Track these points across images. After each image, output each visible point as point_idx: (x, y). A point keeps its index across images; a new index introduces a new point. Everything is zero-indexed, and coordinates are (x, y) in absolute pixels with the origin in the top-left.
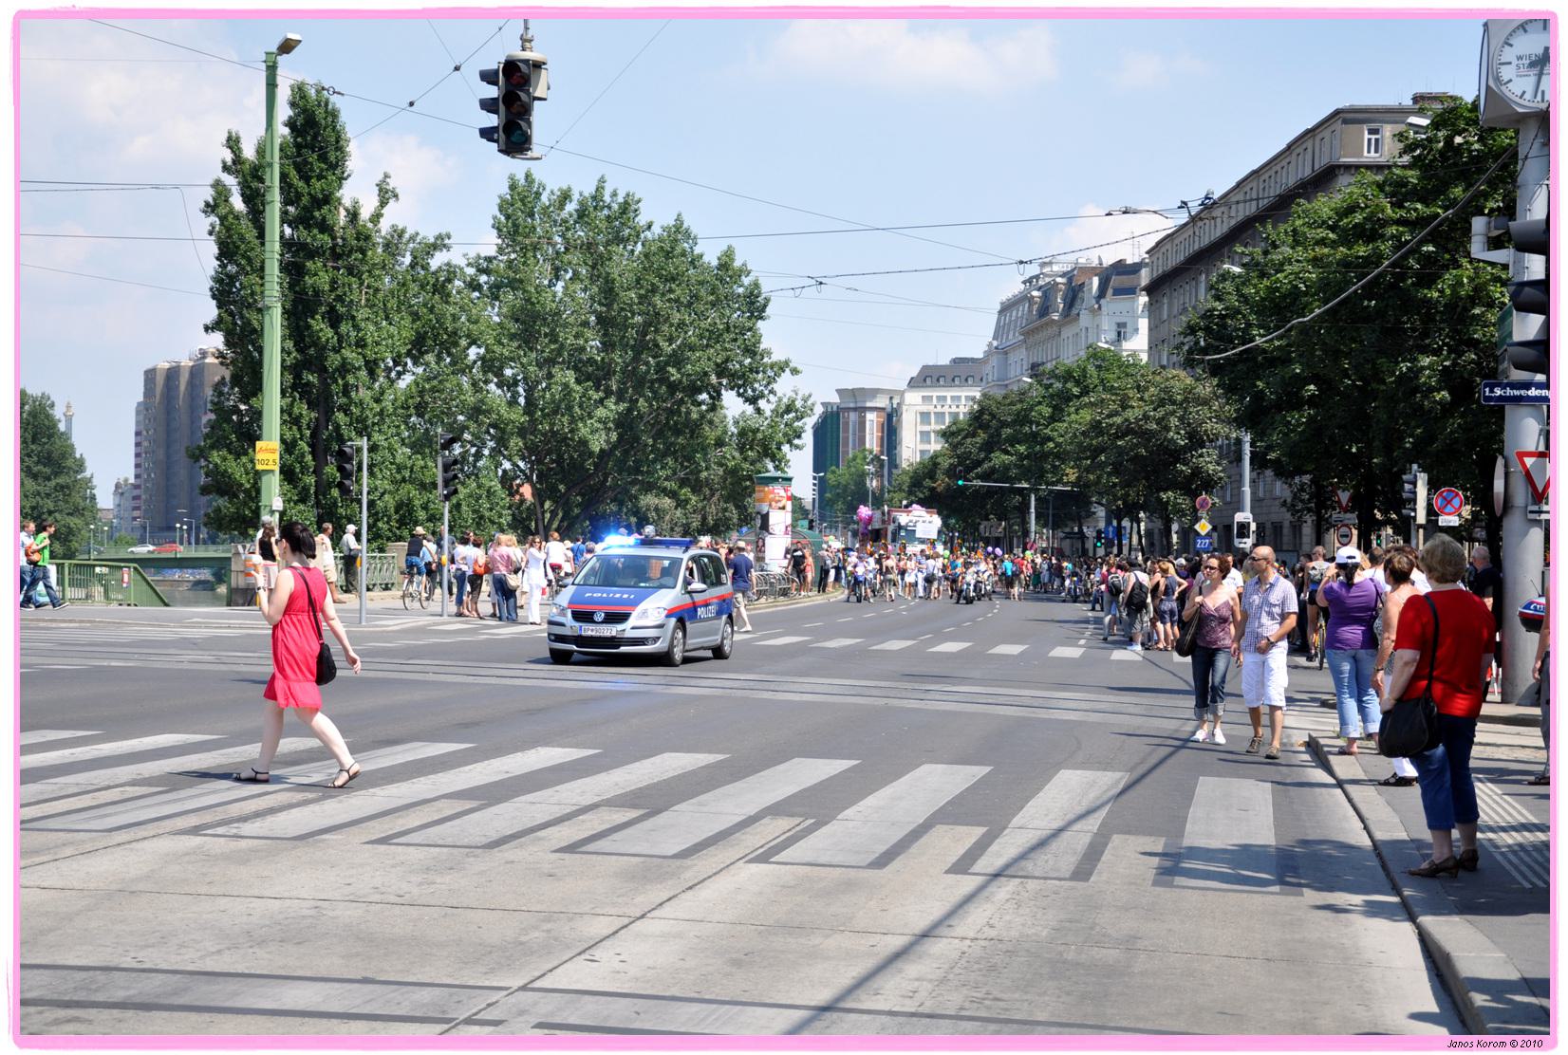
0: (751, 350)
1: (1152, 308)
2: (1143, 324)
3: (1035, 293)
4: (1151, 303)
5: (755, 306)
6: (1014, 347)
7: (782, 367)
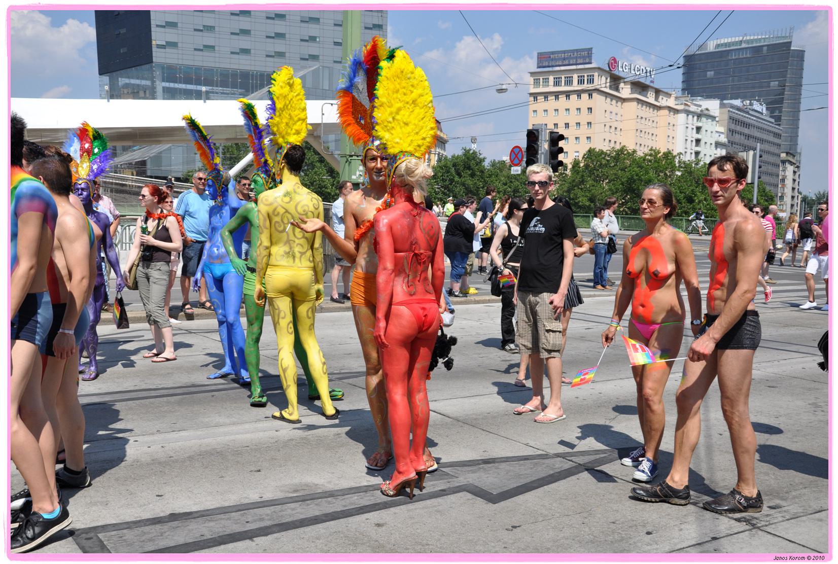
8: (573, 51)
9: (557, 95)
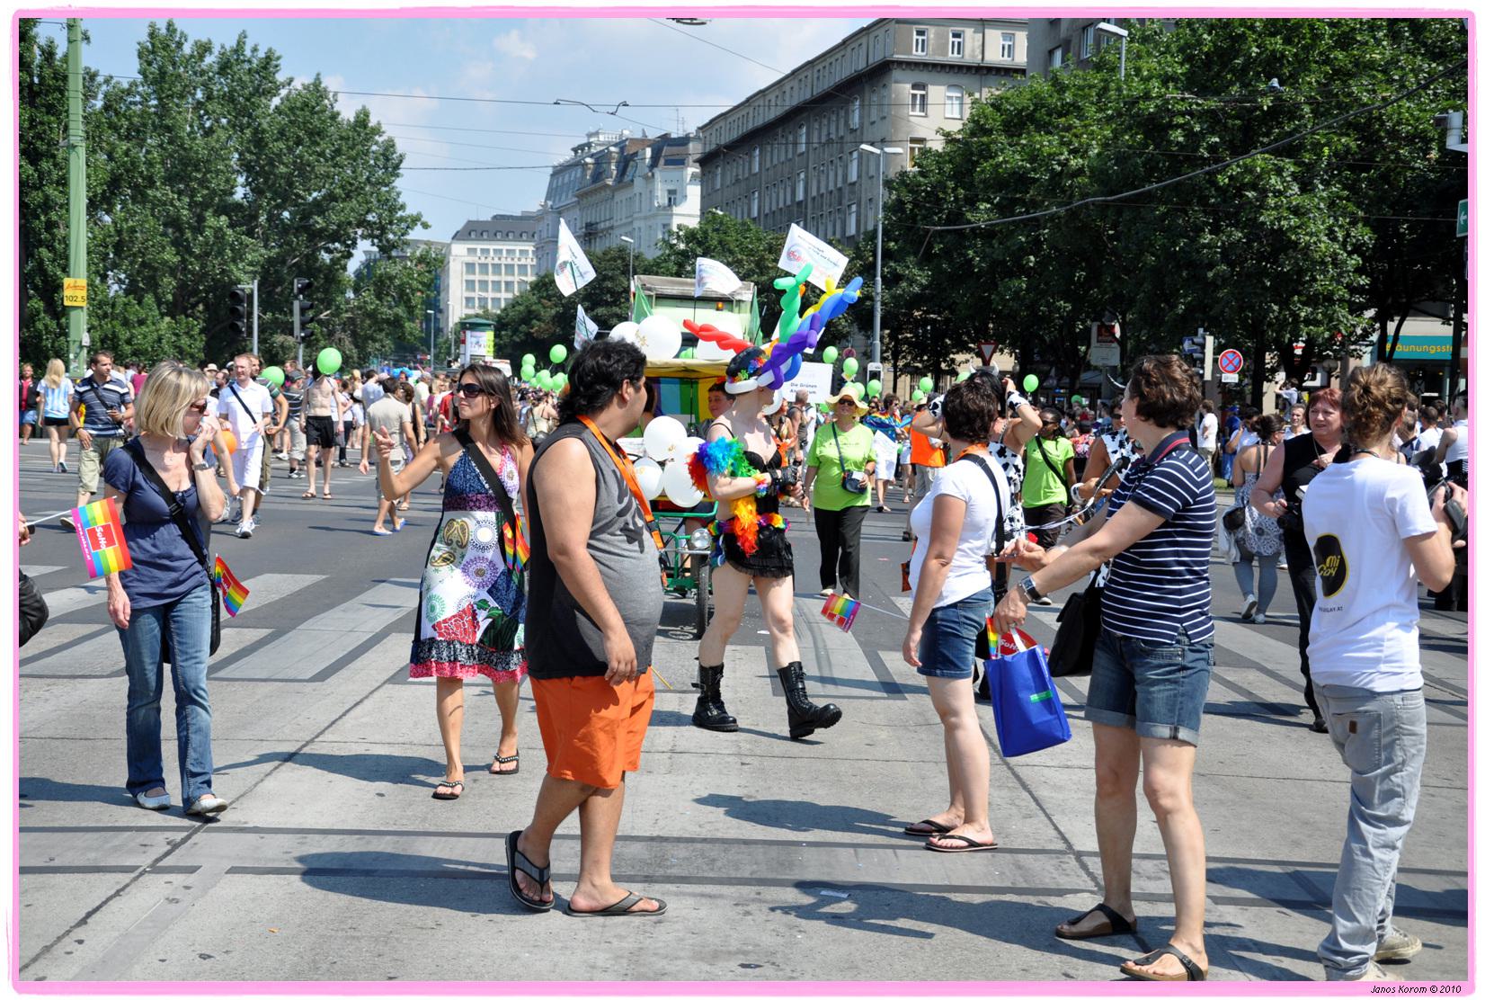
0: (392, 207)
1: (705, 179)
2: (694, 193)
3: (588, 160)
4: (703, 174)
5: (390, 162)
6: (568, 208)
7: (415, 220)
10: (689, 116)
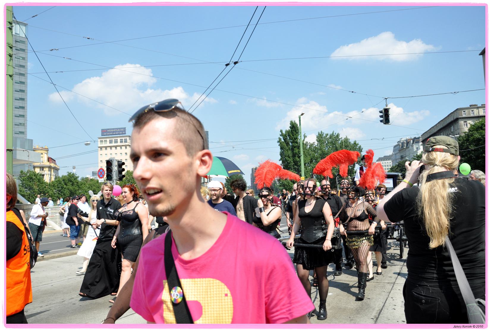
1: (423, 145)
2: (421, 147)
6: (397, 153)
8: (117, 129)
9: (111, 147)
10: (419, 133)
